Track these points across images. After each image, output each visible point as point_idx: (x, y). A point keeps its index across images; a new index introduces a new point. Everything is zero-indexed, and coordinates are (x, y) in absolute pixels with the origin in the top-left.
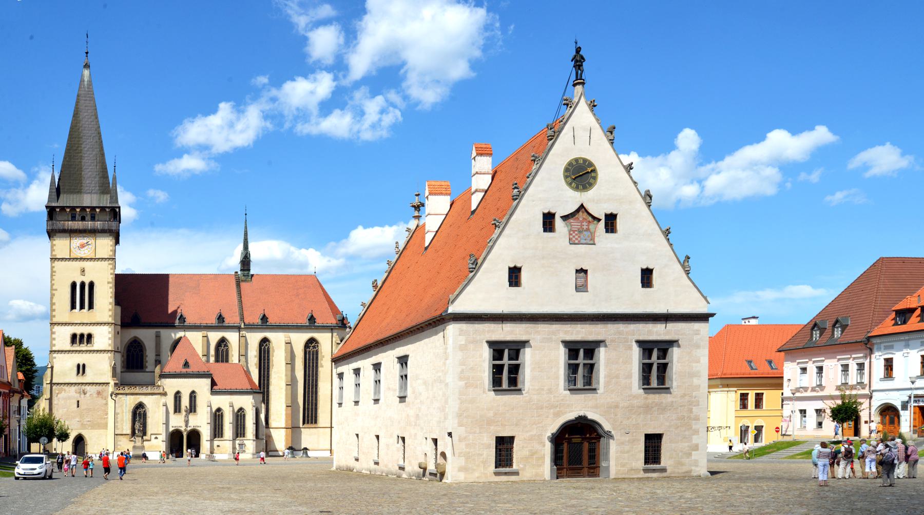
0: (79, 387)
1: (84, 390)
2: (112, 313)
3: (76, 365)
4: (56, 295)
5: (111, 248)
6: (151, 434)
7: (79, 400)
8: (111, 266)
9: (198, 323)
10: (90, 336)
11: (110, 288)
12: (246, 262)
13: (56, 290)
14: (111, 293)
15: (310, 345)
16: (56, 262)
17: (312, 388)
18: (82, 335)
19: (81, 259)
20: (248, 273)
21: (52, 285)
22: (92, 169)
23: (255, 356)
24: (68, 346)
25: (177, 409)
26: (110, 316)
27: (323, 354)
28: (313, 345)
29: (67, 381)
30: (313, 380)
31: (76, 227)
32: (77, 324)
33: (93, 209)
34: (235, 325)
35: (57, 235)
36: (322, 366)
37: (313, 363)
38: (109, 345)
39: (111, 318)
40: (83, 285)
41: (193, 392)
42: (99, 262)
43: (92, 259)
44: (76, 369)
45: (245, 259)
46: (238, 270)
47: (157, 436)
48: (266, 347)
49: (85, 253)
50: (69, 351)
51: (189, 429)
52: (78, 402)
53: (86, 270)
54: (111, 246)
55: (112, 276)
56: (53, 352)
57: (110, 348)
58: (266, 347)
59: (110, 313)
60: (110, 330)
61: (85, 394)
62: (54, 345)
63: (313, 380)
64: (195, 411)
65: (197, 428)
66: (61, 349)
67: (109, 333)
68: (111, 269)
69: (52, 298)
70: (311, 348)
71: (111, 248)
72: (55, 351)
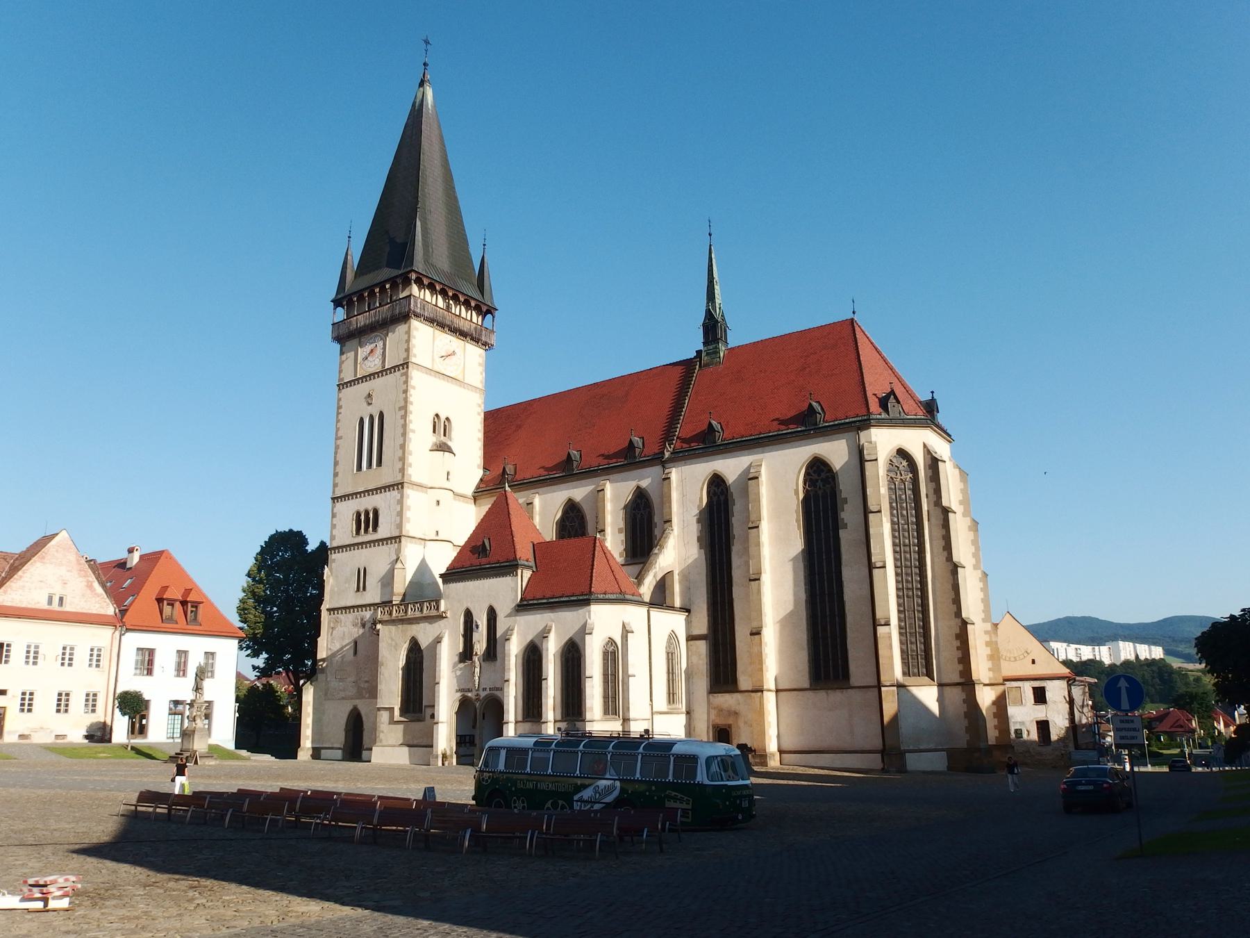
6: (425, 706)
10: (376, 512)
12: (713, 328)
13: (341, 438)
19: (370, 375)
20: (716, 347)
21: (338, 430)
28: (823, 475)
29: (343, 604)
32: (360, 493)
35: (348, 344)
36: (845, 526)
46: (701, 347)
48: (722, 498)
49: (374, 365)
50: (349, 546)
51: (483, 694)
58: (722, 498)
65: (498, 693)
66: (340, 544)
69: (336, 453)
70: (820, 483)
72: (334, 548)
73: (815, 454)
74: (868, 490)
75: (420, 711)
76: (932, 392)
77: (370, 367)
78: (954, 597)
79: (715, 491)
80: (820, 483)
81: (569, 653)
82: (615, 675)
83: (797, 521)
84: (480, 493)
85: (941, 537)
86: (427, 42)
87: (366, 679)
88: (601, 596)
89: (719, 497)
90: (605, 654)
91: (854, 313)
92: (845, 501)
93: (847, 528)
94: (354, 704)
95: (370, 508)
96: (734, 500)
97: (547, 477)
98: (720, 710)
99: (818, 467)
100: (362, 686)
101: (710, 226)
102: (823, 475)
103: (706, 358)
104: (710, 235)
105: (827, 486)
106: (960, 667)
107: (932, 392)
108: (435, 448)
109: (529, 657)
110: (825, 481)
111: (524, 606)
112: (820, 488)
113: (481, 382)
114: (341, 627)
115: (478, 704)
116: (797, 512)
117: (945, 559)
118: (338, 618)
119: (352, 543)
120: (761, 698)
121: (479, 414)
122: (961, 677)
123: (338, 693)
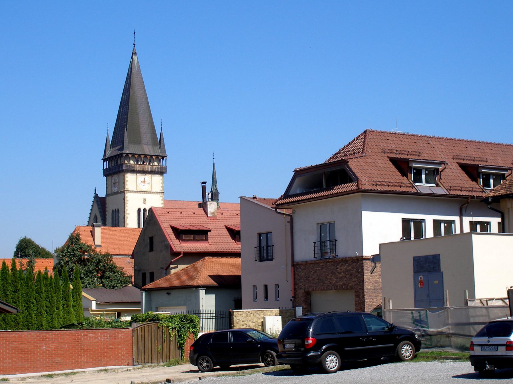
4: (128, 218)
5: (161, 185)
8: (162, 198)
13: (129, 214)
16: (128, 193)
22: (146, 127)
33: (151, 156)
40: (145, 210)
43: (150, 192)
45: (215, 191)
49: (146, 188)
54: (161, 183)
68: (162, 200)
71: (161, 185)
104: (214, 159)
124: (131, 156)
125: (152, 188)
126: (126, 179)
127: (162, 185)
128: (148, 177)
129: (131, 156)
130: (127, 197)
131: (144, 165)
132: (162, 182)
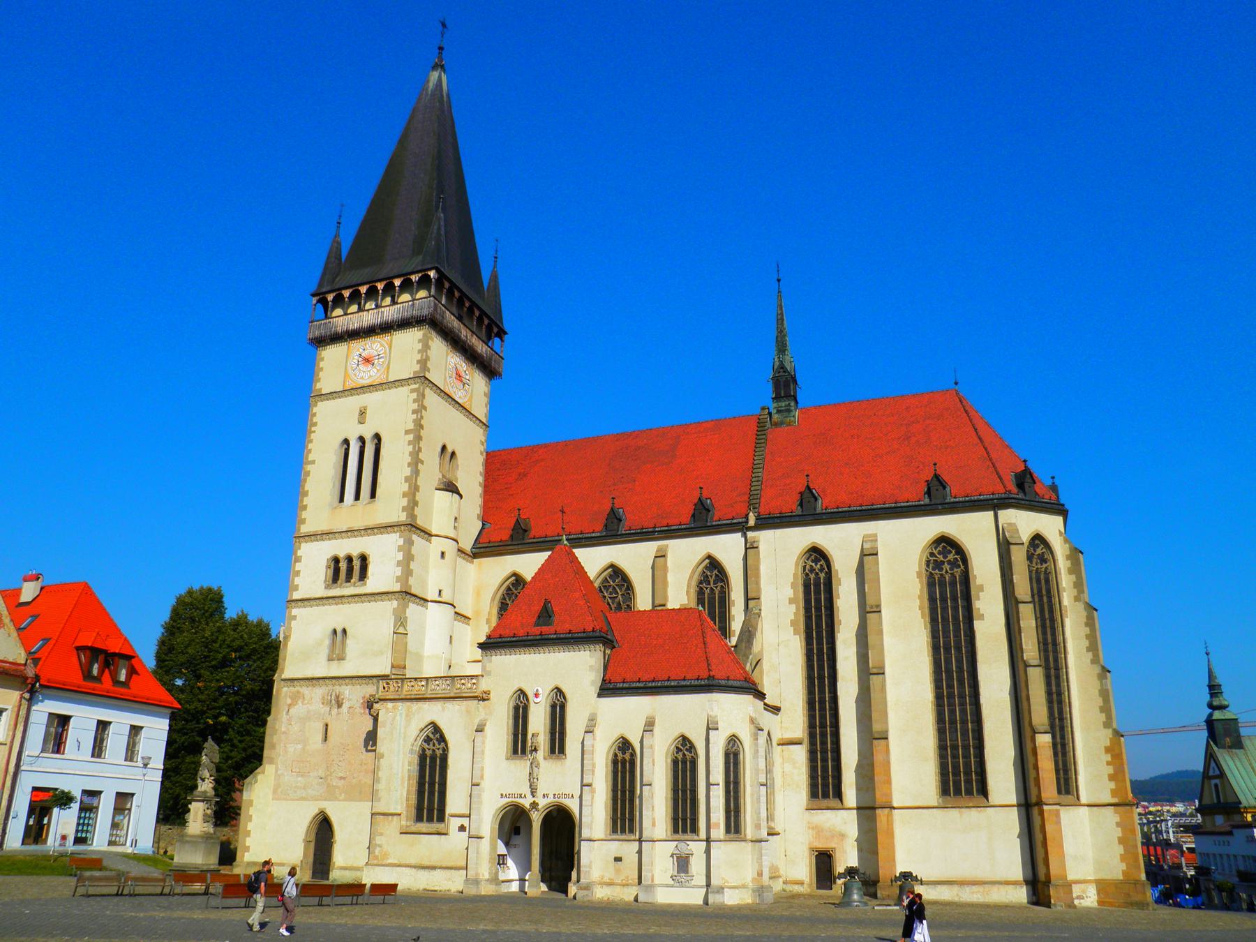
0: (330, 687)
1: (337, 697)
2: (409, 501)
3: (330, 630)
7: (328, 720)
8: (414, 395)
9: (648, 524)
10: (364, 559)
11: (410, 443)
12: (785, 385)
13: (313, 462)
14: (411, 453)
15: (941, 558)
16: (319, 404)
17: (961, 682)
18: (349, 559)
20: (789, 404)
23: (791, 601)
24: (321, 592)
25: (520, 744)
26: (404, 509)
27: (979, 581)
28: (951, 557)
29: (309, 675)
30: (959, 661)
31: (356, 325)
34: (735, 521)
36: (981, 617)
37: (955, 608)
38: (398, 579)
39: (405, 513)
41: (559, 691)
42: (393, 391)
44: (327, 642)
47: (465, 822)
48: (822, 575)
49: (368, 375)
51: (542, 803)
52: (327, 725)
53: (368, 411)
54: (419, 351)
55: (415, 415)
56: (293, 604)
57: (397, 587)
59: (405, 502)
60: (401, 542)
61: (339, 706)
62: (296, 588)
63: (959, 661)
64: (562, 750)
67: (400, 549)
68: (415, 401)
70: (946, 567)
71: (419, 357)
73: (942, 532)
74: (1014, 577)
75: (441, 818)
76: (1053, 478)
77: (362, 378)
78: (1102, 704)
79: (811, 566)
80: (946, 567)
81: (677, 753)
82: (737, 783)
83: (921, 608)
84: (482, 550)
85: (1085, 637)
86: (444, 25)
87: (342, 775)
88: (723, 682)
89: (817, 574)
90: (727, 755)
91: (956, 383)
92: (981, 588)
93: (983, 620)
94: (323, 807)
95: (355, 553)
96: (840, 579)
97: (580, 536)
98: (818, 830)
99: (944, 547)
100: (334, 784)
101: (778, 271)
102: (951, 557)
103: (776, 416)
104: (779, 280)
105: (955, 570)
106: (1112, 785)
107: (1053, 478)
108: (442, 487)
109: (616, 755)
110: (953, 564)
111: (608, 689)
112: (947, 572)
113: (486, 416)
114: (302, 703)
115: (534, 816)
116: (920, 597)
117: (1089, 661)
118: (298, 692)
119: (325, 596)
120: (890, 817)
121: (482, 454)
122: (1113, 797)
123: (295, 792)
124: (332, 297)
125: (388, 372)
126: (319, 366)
127: (422, 356)
128: (374, 345)
129: (334, 298)
130: (315, 415)
131: (365, 313)
132: (420, 348)
